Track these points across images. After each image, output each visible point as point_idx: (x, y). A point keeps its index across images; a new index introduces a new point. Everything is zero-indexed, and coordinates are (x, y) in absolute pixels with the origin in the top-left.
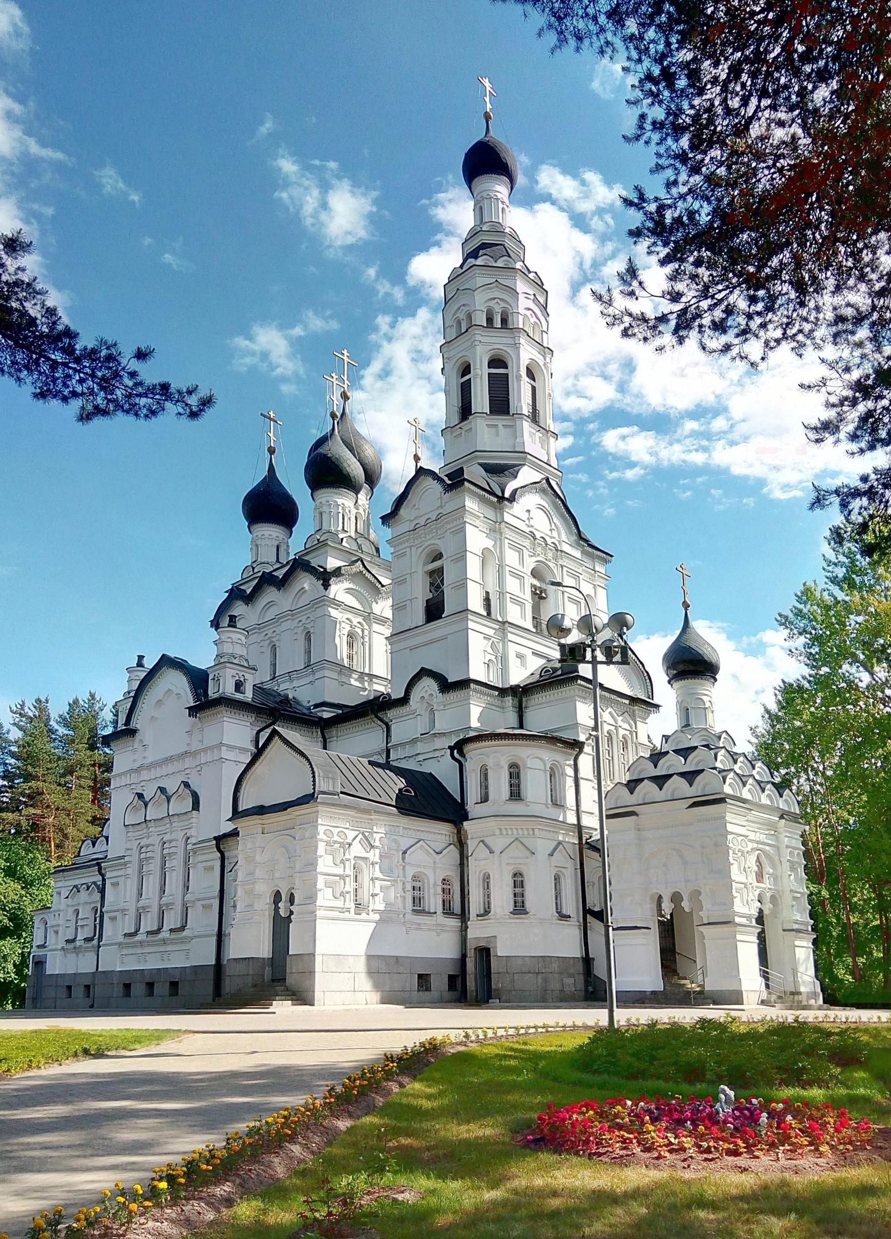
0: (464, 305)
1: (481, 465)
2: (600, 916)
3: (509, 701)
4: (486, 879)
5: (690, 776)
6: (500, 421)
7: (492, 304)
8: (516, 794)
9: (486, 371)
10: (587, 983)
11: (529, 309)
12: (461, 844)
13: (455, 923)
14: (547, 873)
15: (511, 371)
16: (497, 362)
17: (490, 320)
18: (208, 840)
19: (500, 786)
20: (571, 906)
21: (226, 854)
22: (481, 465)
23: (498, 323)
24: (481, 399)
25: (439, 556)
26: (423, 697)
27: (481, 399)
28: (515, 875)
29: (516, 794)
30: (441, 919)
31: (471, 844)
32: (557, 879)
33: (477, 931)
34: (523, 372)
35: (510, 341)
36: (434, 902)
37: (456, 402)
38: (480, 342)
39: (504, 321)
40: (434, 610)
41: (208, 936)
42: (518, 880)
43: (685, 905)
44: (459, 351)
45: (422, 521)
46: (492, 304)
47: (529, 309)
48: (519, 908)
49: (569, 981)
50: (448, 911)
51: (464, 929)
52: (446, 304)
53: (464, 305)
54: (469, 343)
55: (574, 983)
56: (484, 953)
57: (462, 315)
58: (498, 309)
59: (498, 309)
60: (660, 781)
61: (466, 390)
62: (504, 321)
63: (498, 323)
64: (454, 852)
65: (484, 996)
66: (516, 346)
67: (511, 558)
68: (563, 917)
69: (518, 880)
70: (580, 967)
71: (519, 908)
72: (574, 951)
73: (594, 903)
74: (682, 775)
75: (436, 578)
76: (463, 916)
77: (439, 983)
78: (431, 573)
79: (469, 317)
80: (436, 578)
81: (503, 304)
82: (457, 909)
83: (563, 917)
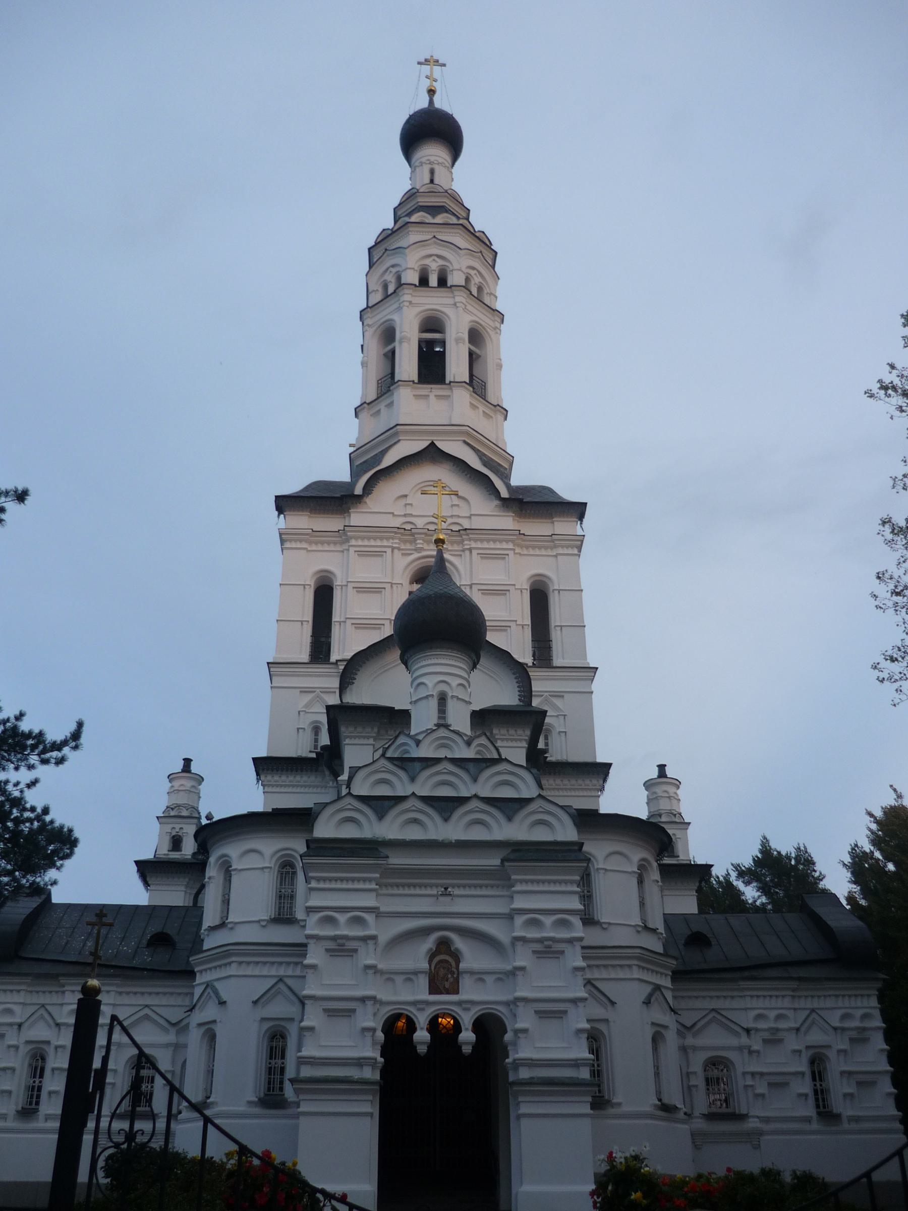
0: (393, 266)
7: (427, 262)
11: (474, 268)
23: (433, 281)
27: (408, 364)
35: (451, 301)
37: (376, 370)
38: (410, 302)
44: (384, 314)
46: (427, 262)
47: (474, 268)
52: (370, 267)
53: (393, 266)
54: (396, 306)
57: (390, 278)
58: (434, 265)
59: (434, 265)
63: (433, 281)
79: (399, 278)
81: (441, 262)
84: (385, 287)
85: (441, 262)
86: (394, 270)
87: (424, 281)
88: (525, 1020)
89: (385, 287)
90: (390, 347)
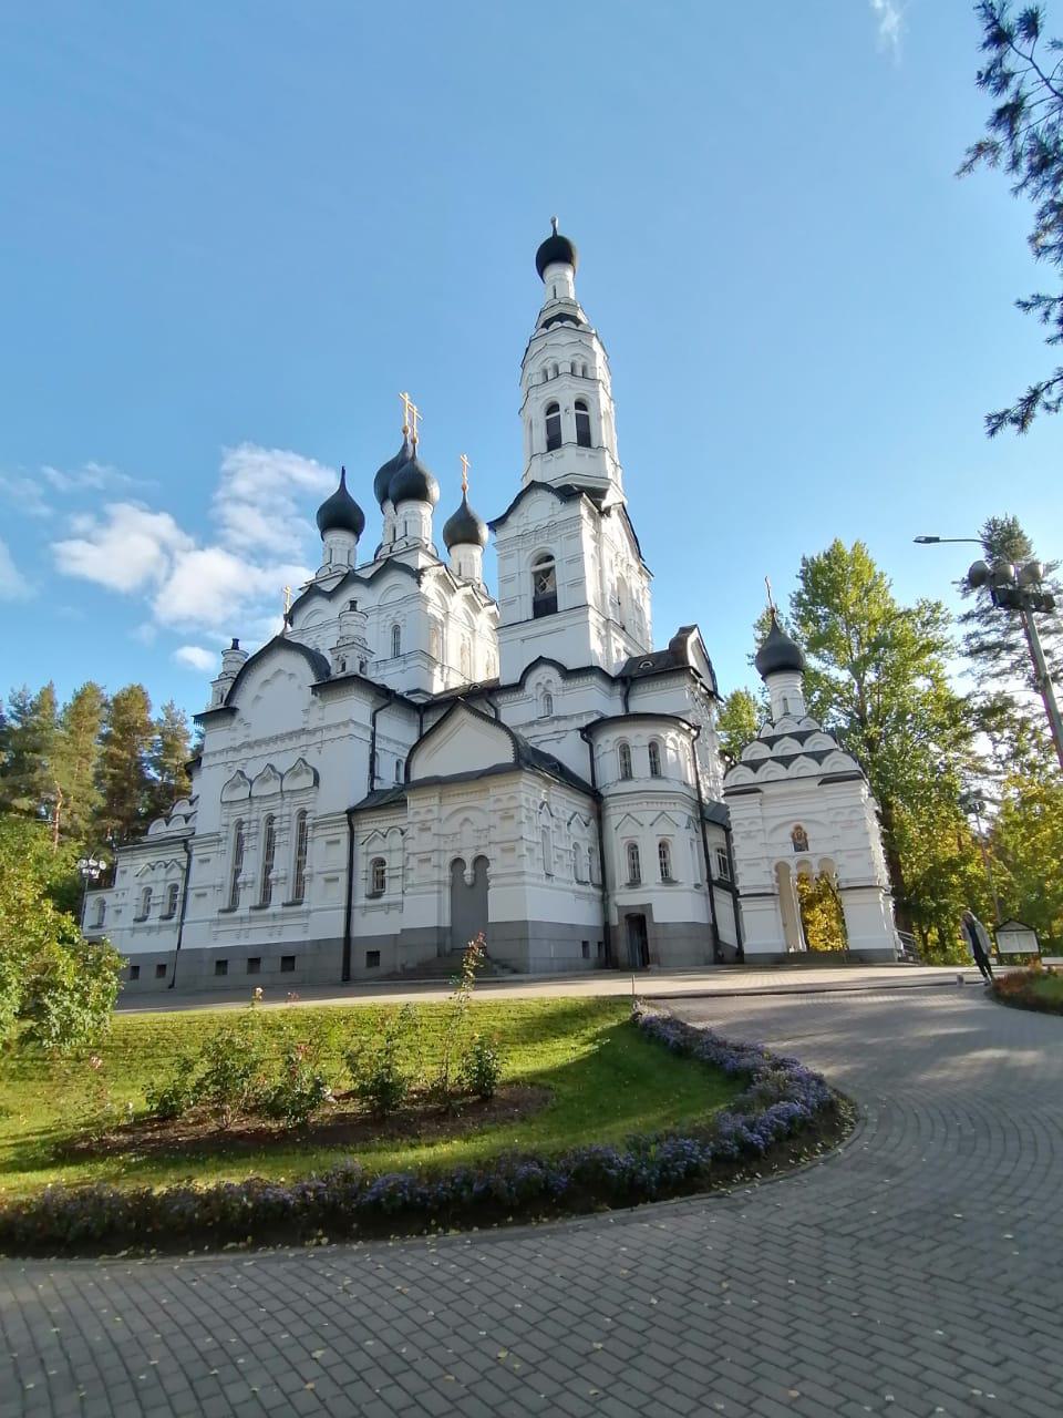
2: (730, 886)
3: (618, 689)
4: (633, 850)
7: (575, 358)
8: (655, 771)
9: (573, 411)
13: (598, 893)
16: (580, 405)
17: (573, 373)
18: (340, 813)
21: (356, 829)
24: (569, 431)
25: (550, 558)
26: (539, 684)
27: (569, 431)
28: (660, 846)
29: (655, 771)
30: (590, 889)
39: (584, 370)
40: (545, 606)
41: (338, 908)
42: (663, 849)
45: (531, 527)
46: (575, 358)
48: (667, 879)
57: (549, 365)
58: (580, 363)
62: (584, 370)
65: (642, 962)
69: (663, 849)
75: (543, 577)
76: (604, 886)
78: (536, 574)
79: (556, 368)
80: (543, 577)
84: (545, 372)
85: (583, 360)
86: (552, 361)
87: (573, 373)
88: (841, 859)
89: (545, 372)
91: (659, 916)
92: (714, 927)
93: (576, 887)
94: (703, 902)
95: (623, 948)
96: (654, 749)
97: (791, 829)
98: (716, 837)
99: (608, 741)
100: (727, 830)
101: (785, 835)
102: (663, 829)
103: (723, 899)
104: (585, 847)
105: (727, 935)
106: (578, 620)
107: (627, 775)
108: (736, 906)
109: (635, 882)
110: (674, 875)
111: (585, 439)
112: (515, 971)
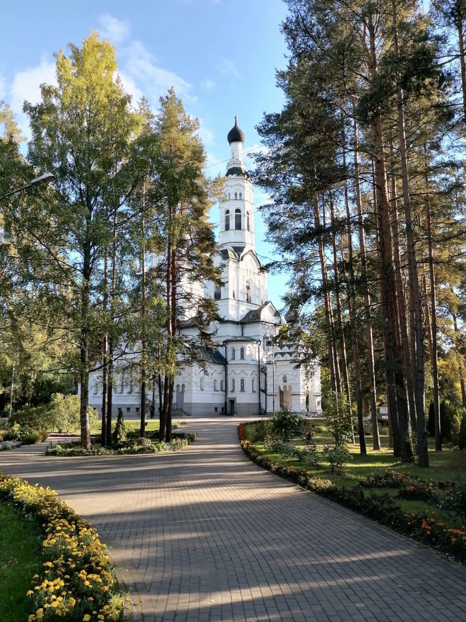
1: (233, 247)
2: (265, 391)
3: (240, 326)
5: (290, 354)
6: (238, 231)
8: (242, 357)
9: (234, 213)
10: (259, 410)
12: (226, 370)
13: (224, 393)
14: (250, 376)
15: (242, 214)
16: (238, 211)
19: (238, 354)
20: (256, 389)
22: (233, 247)
23: (238, 197)
29: (242, 357)
31: (229, 372)
32: (253, 381)
33: (230, 395)
34: (246, 214)
35: (242, 204)
36: (218, 388)
42: (242, 380)
43: (287, 389)
48: (242, 390)
49: (255, 409)
50: (222, 390)
51: (226, 395)
55: (256, 410)
56: (232, 402)
60: (283, 354)
61: (227, 219)
64: (224, 372)
65: (232, 414)
66: (244, 206)
67: (241, 278)
68: (254, 392)
70: (258, 406)
71: (242, 390)
72: (257, 402)
73: (263, 387)
74: (288, 353)
76: (226, 391)
77: (220, 410)
82: (224, 389)
83: (254, 392)
90: (228, 215)
91: (238, 401)
92: (260, 404)
93: (213, 392)
94: (256, 396)
95: (228, 410)
96: (242, 350)
97: (283, 376)
98: (263, 376)
99: (230, 346)
100: (266, 375)
101: (281, 378)
102: (242, 375)
103: (263, 395)
104: (219, 381)
105: (263, 406)
106: (226, 303)
107: (234, 359)
108: (266, 398)
109: (233, 391)
110: (245, 388)
111: (238, 226)
112: (189, 415)
